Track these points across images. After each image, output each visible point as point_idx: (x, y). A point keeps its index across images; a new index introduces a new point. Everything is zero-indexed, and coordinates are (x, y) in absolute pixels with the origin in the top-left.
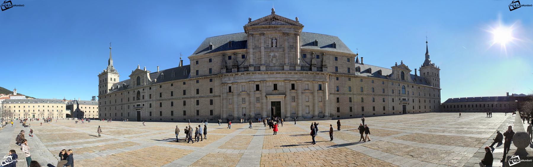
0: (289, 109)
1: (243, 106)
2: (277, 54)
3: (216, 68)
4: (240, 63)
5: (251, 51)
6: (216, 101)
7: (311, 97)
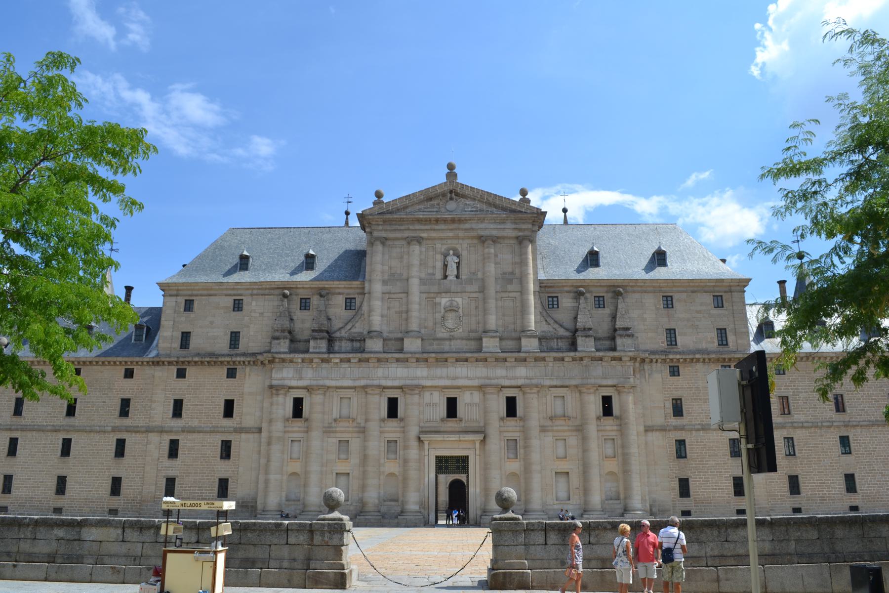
1: (342, 468)
3: (254, 337)
4: (337, 324)
5: (377, 288)
6: (243, 446)
7: (573, 441)
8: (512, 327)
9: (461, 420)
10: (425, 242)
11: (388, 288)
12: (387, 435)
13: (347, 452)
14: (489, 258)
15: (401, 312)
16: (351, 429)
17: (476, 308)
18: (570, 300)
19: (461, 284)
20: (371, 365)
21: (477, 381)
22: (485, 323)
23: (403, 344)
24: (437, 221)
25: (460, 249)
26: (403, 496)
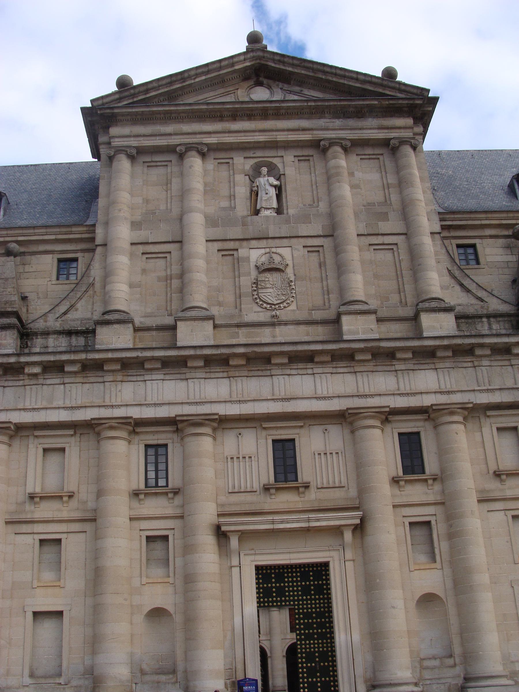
0: (399, 614)
2: (286, 252)
5: (123, 233)
8: (395, 298)
9: (307, 487)
10: (212, 155)
11: (143, 235)
12: (145, 525)
13: (57, 565)
14: (338, 174)
15: (168, 278)
16: (65, 514)
17: (321, 265)
18: (501, 251)
19: (288, 221)
20: (109, 378)
21: (336, 401)
22: (342, 290)
23: (176, 335)
24: (235, 115)
25: (280, 166)
26: (186, 659)
